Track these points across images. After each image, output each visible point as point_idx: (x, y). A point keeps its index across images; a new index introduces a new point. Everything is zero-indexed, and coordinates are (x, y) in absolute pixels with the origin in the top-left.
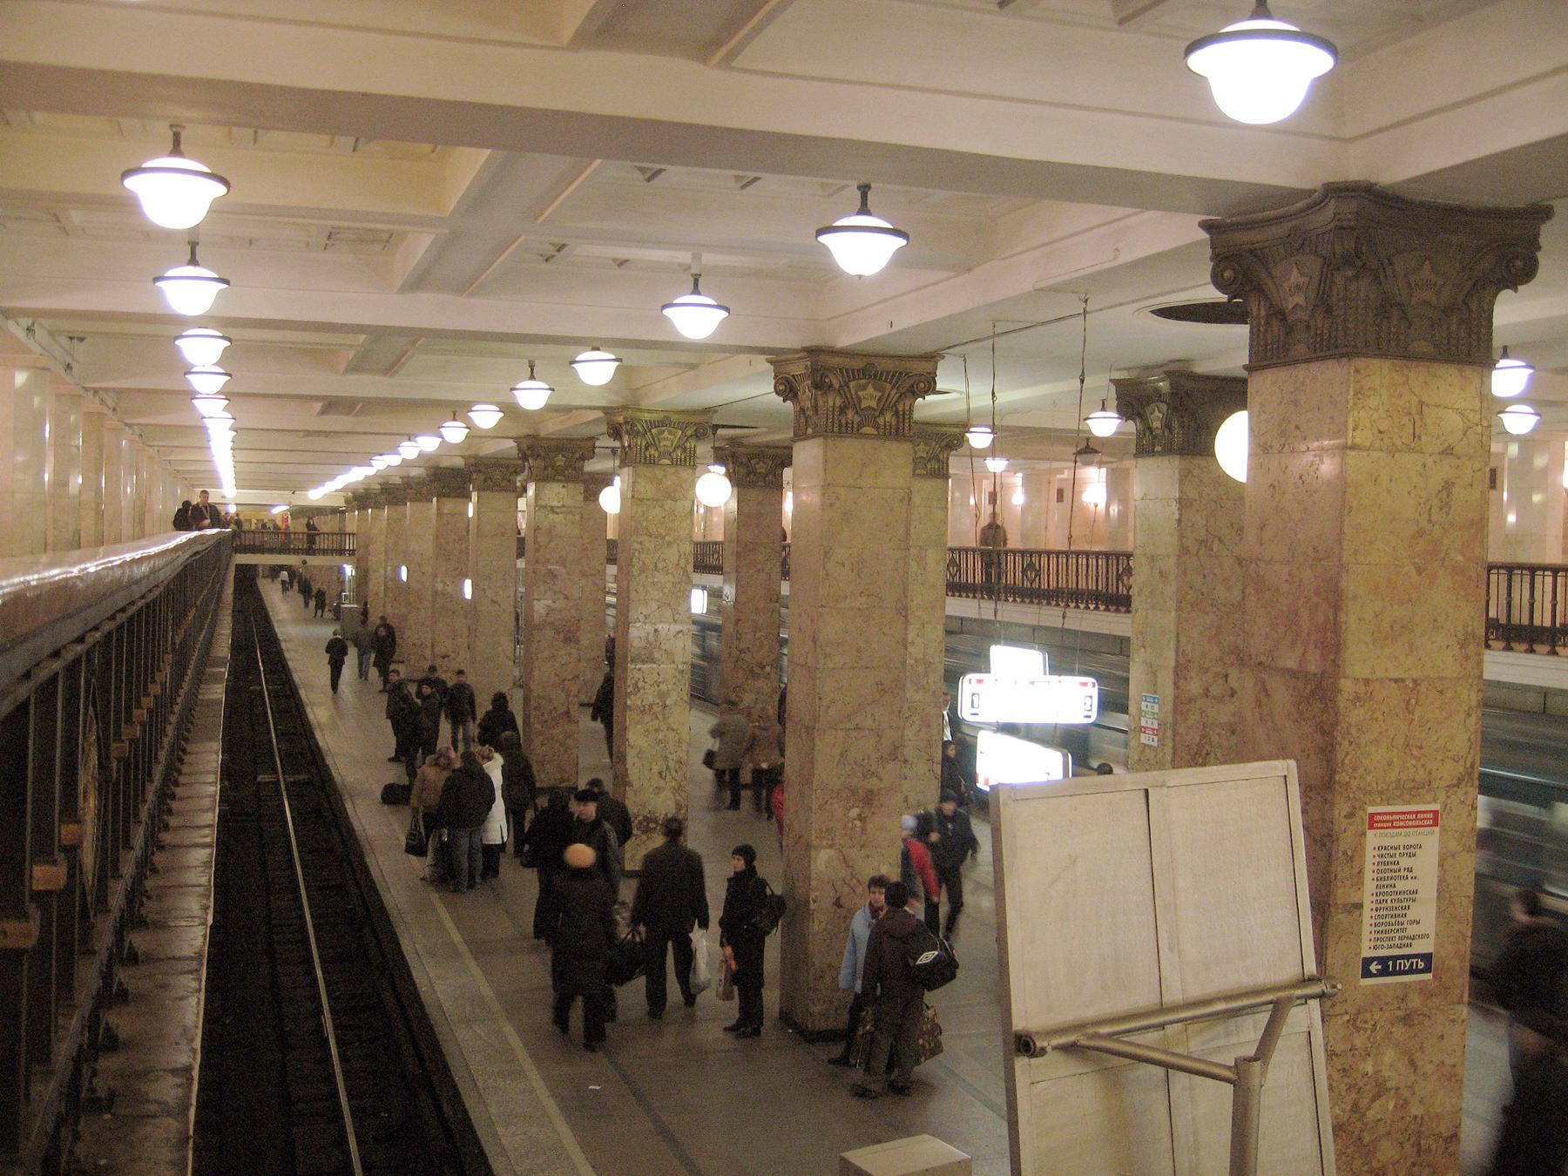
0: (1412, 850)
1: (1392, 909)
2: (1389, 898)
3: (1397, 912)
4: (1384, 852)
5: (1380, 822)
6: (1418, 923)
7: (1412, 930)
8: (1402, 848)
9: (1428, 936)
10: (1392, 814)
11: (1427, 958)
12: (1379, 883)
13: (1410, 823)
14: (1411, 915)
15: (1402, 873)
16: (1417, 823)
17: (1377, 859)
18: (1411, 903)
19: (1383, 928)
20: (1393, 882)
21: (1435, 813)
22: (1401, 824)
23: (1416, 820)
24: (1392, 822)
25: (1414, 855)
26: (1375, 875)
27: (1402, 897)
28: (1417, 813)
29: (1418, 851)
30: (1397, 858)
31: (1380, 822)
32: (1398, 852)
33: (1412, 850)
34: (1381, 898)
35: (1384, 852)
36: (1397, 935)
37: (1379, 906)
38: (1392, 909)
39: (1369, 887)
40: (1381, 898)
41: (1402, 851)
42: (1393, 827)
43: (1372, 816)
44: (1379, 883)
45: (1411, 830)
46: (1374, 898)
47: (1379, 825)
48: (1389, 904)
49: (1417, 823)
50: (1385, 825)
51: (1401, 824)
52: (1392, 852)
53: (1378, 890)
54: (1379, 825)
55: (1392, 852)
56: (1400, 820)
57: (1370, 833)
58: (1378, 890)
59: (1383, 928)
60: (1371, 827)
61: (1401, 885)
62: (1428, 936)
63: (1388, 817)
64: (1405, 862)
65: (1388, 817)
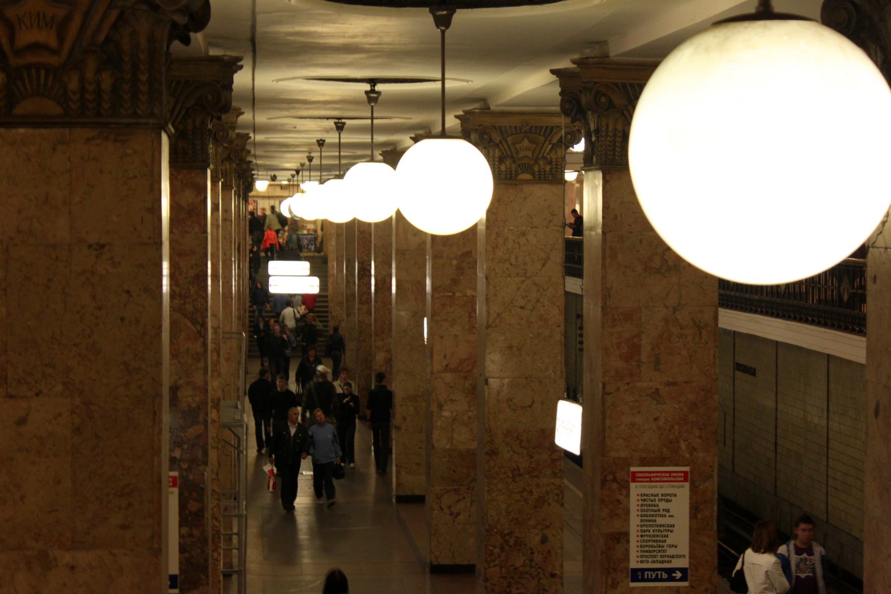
0: (669, 497)
1: (654, 536)
2: (651, 529)
3: (658, 539)
4: (645, 497)
5: (641, 477)
6: (676, 547)
7: (671, 551)
8: (660, 495)
9: (684, 556)
10: (650, 472)
11: (683, 571)
12: (643, 518)
13: (665, 479)
14: (669, 541)
15: (661, 512)
16: (671, 479)
17: (641, 502)
18: (669, 533)
19: (647, 549)
20: (653, 518)
21: (685, 473)
22: (658, 479)
23: (671, 478)
24: (650, 477)
25: (670, 501)
26: (639, 513)
27: (662, 529)
28: (670, 472)
29: (673, 498)
30: (657, 502)
31: (641, 477)
32: (657, 498)
33: (669, 497)
34: (645, 528)
35: (645, 497)
36: (659, 554)
37: (643, 534)
38: (654, 536)
39: (634, 521)
40: (645, 528)
41: (660, 497)
42: (651, 481)
43: (634, 473)
44: (643, 518)
45: (666, 484)
46: (639, 528)
47: (640, 479)
48: (652, 533)
49: (671, 479)
50: (645, 480)
51: (658, 479)
52: (652, 498)
53: (643, 523)
54: (640, 479)
55: (652, 498)
56: (656, 477)
57: (633, 485)
58: (643, 523)
59: (647, 549)
60: (634, 481)
61: (660, 520)
62: (684, 556)
63: (647, 475)
64: (663, 505)
65: (647, 475)
